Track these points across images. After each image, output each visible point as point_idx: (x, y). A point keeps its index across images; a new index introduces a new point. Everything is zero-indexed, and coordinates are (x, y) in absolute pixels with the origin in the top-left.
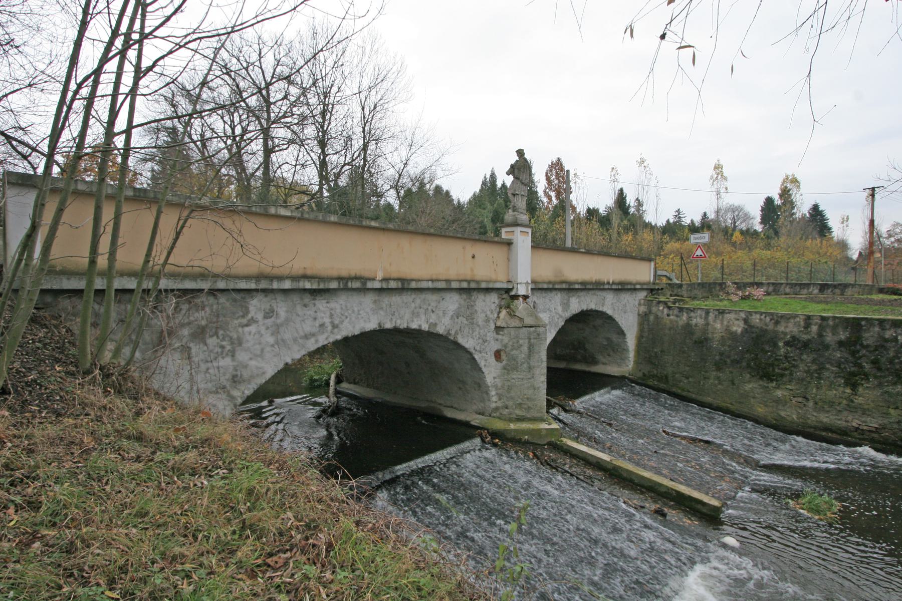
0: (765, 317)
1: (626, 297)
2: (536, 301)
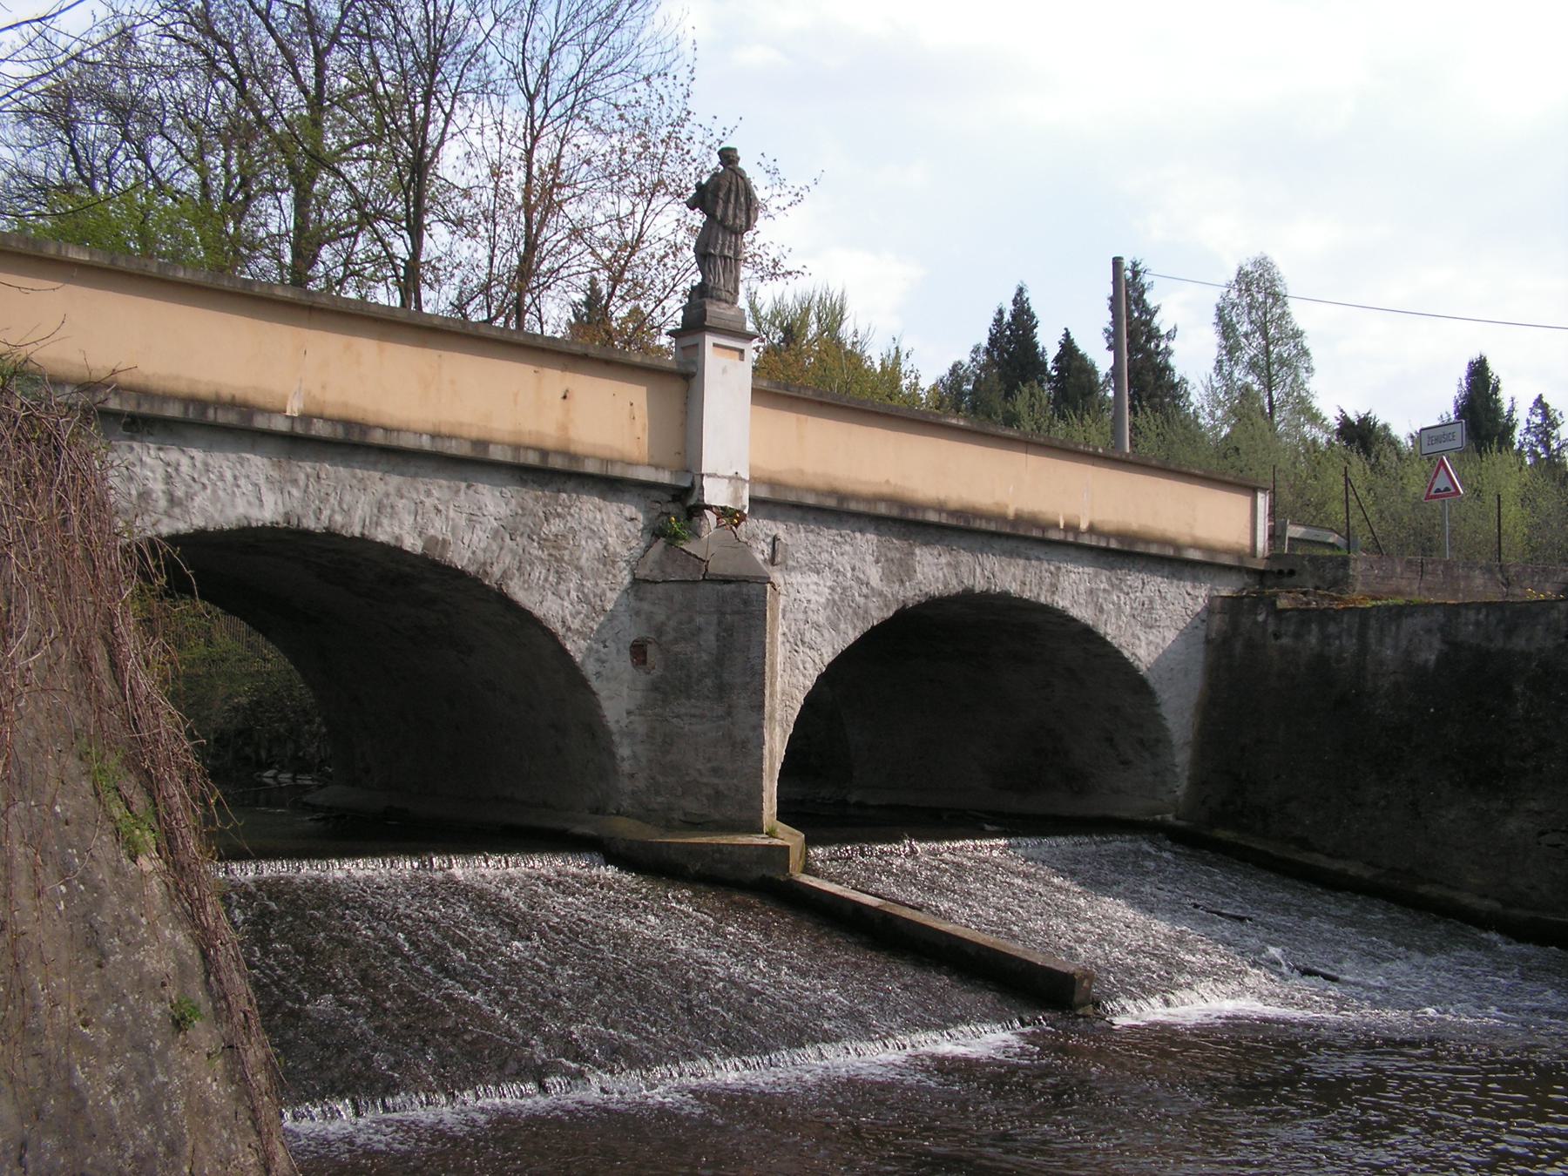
0: (1487, 616)
1: (1156, 586)
2: (782, 534)
